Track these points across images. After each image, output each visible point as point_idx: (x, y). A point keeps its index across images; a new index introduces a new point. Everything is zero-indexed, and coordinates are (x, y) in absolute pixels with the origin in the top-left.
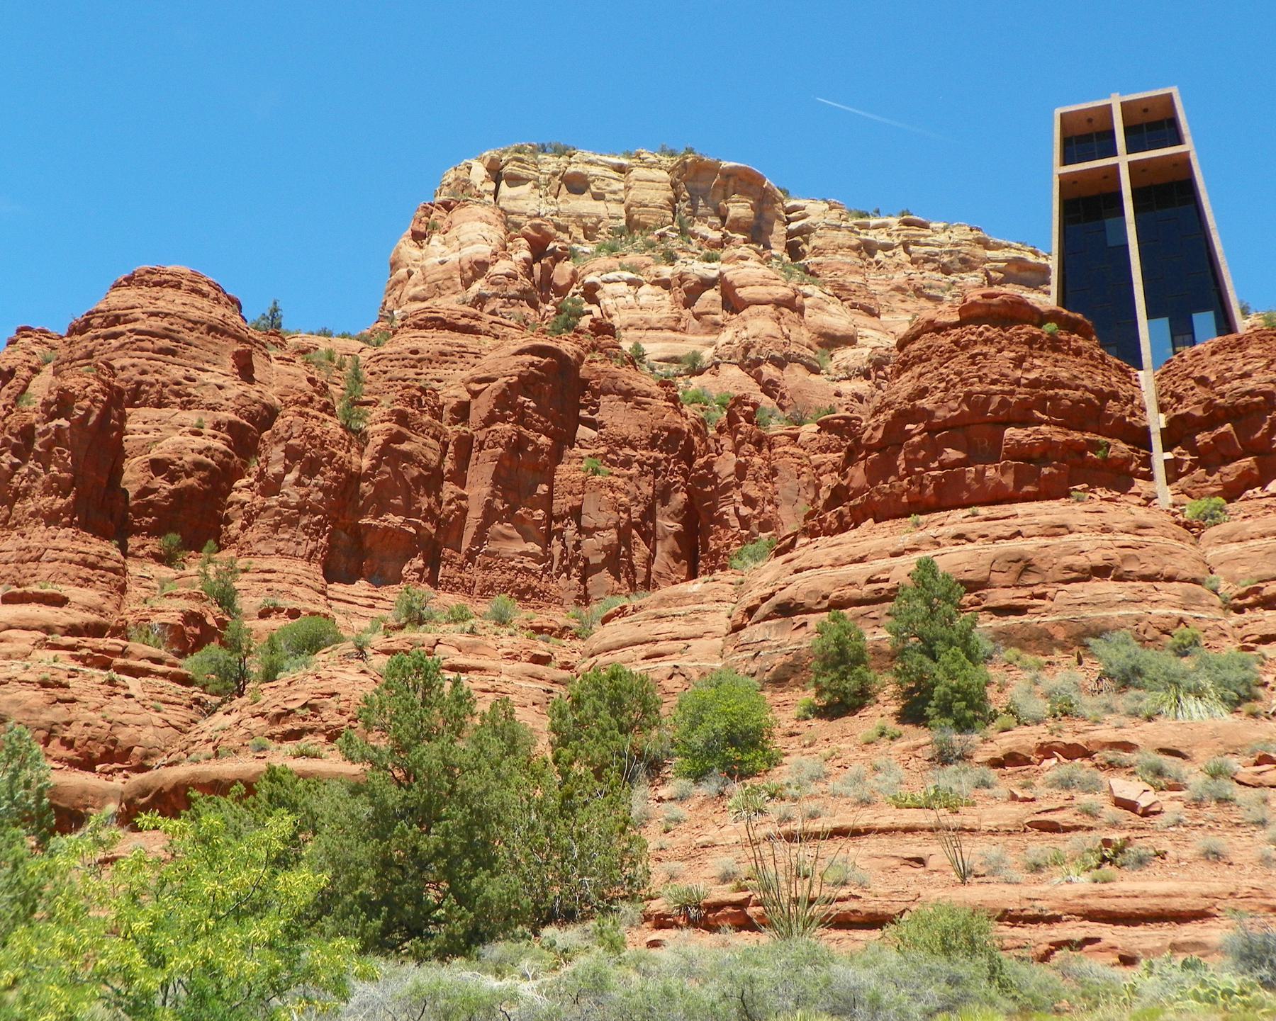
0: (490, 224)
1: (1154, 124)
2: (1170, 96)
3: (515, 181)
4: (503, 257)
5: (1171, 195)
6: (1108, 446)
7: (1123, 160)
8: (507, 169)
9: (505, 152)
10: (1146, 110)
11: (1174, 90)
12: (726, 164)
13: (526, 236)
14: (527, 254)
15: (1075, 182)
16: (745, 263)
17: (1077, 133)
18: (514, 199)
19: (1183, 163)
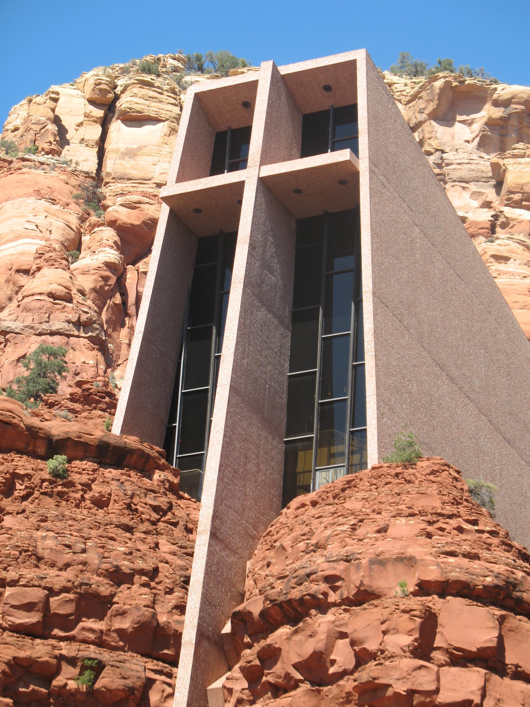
0: (53, 201)
1: (321, 114)
2: (351, 66)
3: (136, 120)
4: (51, 263)
5: (318, 236)
6: (99, 667)
7: (248, 178)
8: (123, 103)
9: (125, 71)
10: (327, 88)
11: (359, 56)
12: (504, 90)
13: (112, 224)
14: (113, 255)
15: (198, 211)
16: (502, 267)
17: (235, 126)
18: (131, 154)
19: (347, 177)
